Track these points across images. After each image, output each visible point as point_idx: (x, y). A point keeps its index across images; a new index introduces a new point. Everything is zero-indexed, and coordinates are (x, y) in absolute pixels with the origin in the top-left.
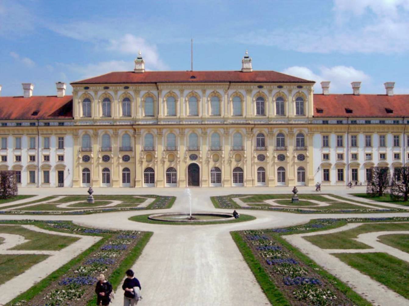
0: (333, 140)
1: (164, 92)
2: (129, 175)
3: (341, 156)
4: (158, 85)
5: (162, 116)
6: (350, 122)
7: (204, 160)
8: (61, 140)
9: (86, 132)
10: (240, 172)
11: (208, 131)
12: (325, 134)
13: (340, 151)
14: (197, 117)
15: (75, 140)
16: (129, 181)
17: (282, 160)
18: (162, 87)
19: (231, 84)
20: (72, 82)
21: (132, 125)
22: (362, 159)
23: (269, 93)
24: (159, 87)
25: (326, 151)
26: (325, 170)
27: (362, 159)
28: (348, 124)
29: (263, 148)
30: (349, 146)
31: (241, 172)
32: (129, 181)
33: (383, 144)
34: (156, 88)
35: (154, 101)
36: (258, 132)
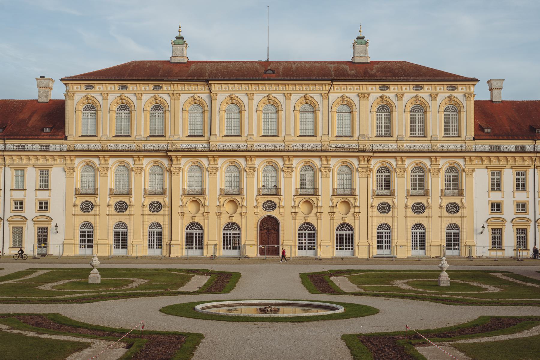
2: (160, 235)
5: (218, 135)
7: (288, 210)
8: (44, 176)
13: (521, 197)
17: (420, 213)
19: (334, 83)
20: (63, 77)
21: (166, 152)
25: (496, 197)
26: (493, 230)
29: (387, 192)
36: (379, 165)
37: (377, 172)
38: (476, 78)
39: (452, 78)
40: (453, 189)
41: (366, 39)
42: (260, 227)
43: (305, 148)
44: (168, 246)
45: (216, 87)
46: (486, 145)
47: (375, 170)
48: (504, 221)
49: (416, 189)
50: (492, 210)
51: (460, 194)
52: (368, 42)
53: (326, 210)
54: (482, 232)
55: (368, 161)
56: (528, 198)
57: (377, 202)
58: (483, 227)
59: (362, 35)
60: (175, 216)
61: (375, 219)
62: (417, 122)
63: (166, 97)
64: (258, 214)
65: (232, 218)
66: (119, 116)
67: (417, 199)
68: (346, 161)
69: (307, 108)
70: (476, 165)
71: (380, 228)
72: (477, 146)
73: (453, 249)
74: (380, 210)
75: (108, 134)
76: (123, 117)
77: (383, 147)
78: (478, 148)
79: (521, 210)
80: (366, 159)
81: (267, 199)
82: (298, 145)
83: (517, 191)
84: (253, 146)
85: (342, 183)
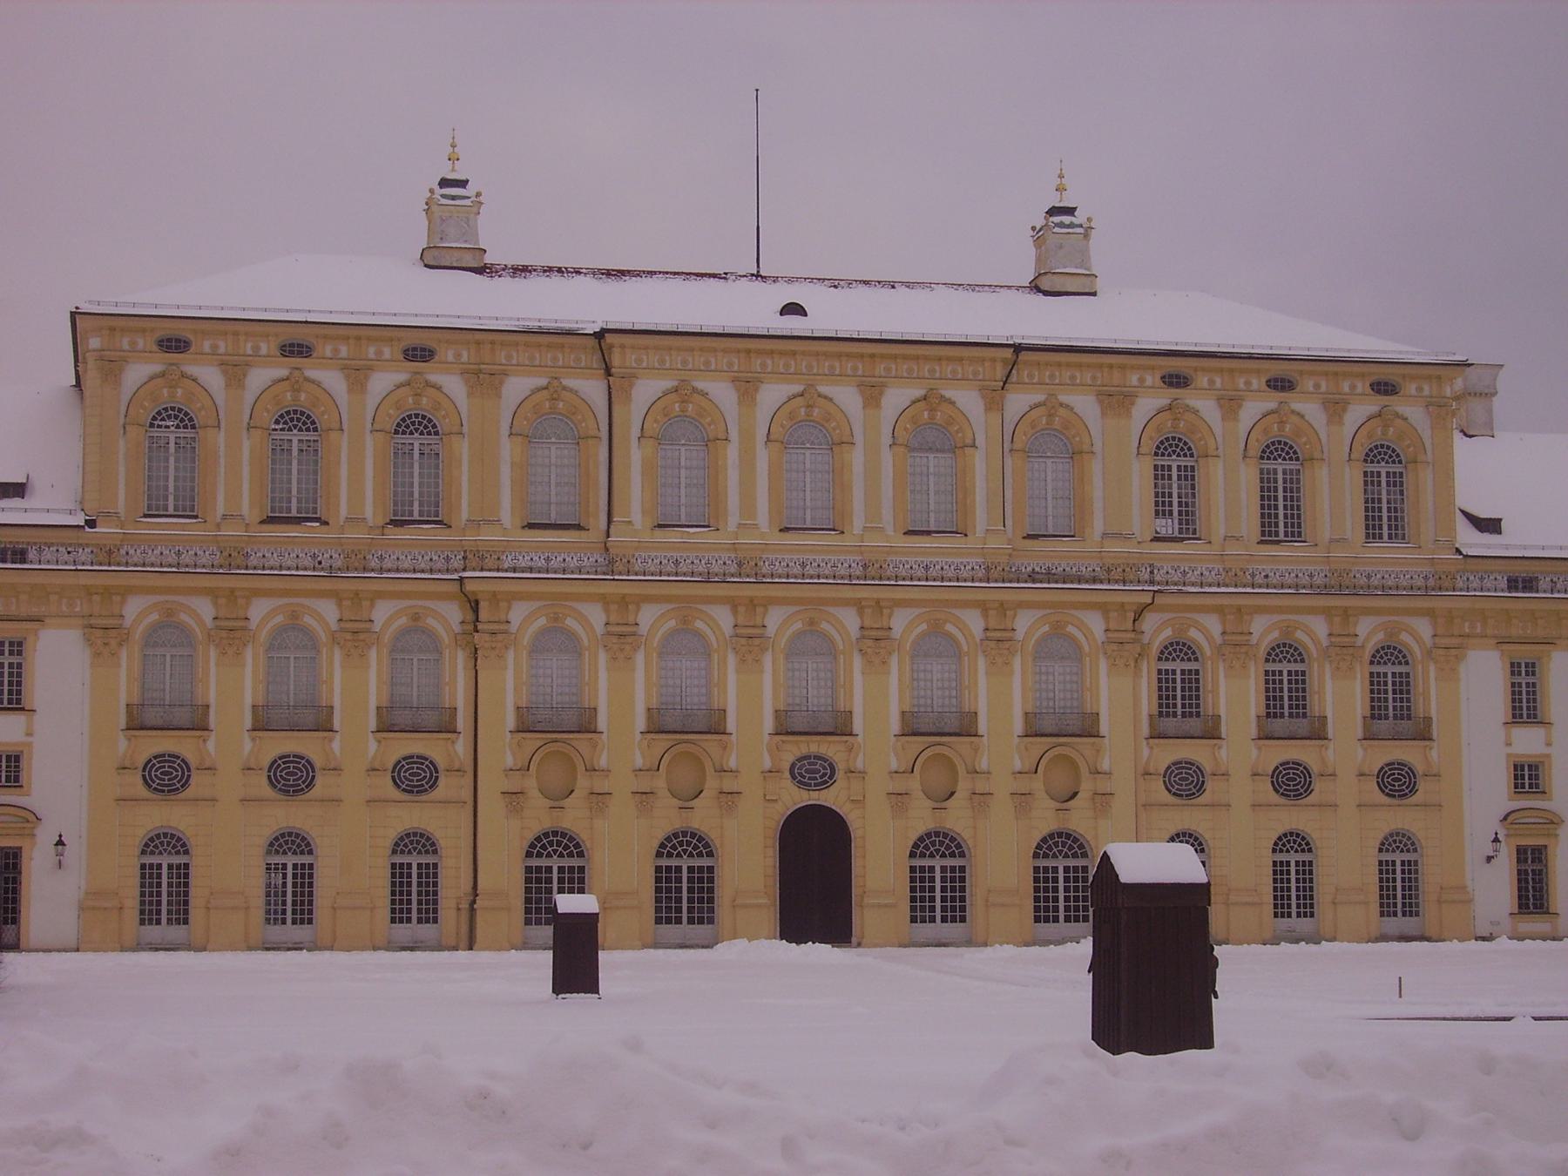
1: (647, 390)
2: (430, 874)
4: (611, 347)
9: (294, 615)
10: (1071, 863)
11: (900, 621)
12: (1524, 653)
14: (831, 539)
15: (97, 654)
16: (429, 914)
17: (1298, 796)
18: (631, 359)
23: (1330, 422)
24: (616, 360)
26: (1521, 852)
32: (429, 914)
34: (596, 361)
35: (580, 440)
36: (1167, 633)
37: (1160, 659)
44: (465, 916)
49: (1282, 715)
54: (1489, 859)
55: (1134, 621)
58: (1496, 840)
60: (490, 805)
62: (1280, 494)
63: (454, 385)
66: (280, 451)
72: (1472, 578)
73: (1400, 914)
74: (1173, 787)
75: (245, 510)
76: (295, 452)
81: (804, 751)
84: (884, 566)
85: (1051, 695)
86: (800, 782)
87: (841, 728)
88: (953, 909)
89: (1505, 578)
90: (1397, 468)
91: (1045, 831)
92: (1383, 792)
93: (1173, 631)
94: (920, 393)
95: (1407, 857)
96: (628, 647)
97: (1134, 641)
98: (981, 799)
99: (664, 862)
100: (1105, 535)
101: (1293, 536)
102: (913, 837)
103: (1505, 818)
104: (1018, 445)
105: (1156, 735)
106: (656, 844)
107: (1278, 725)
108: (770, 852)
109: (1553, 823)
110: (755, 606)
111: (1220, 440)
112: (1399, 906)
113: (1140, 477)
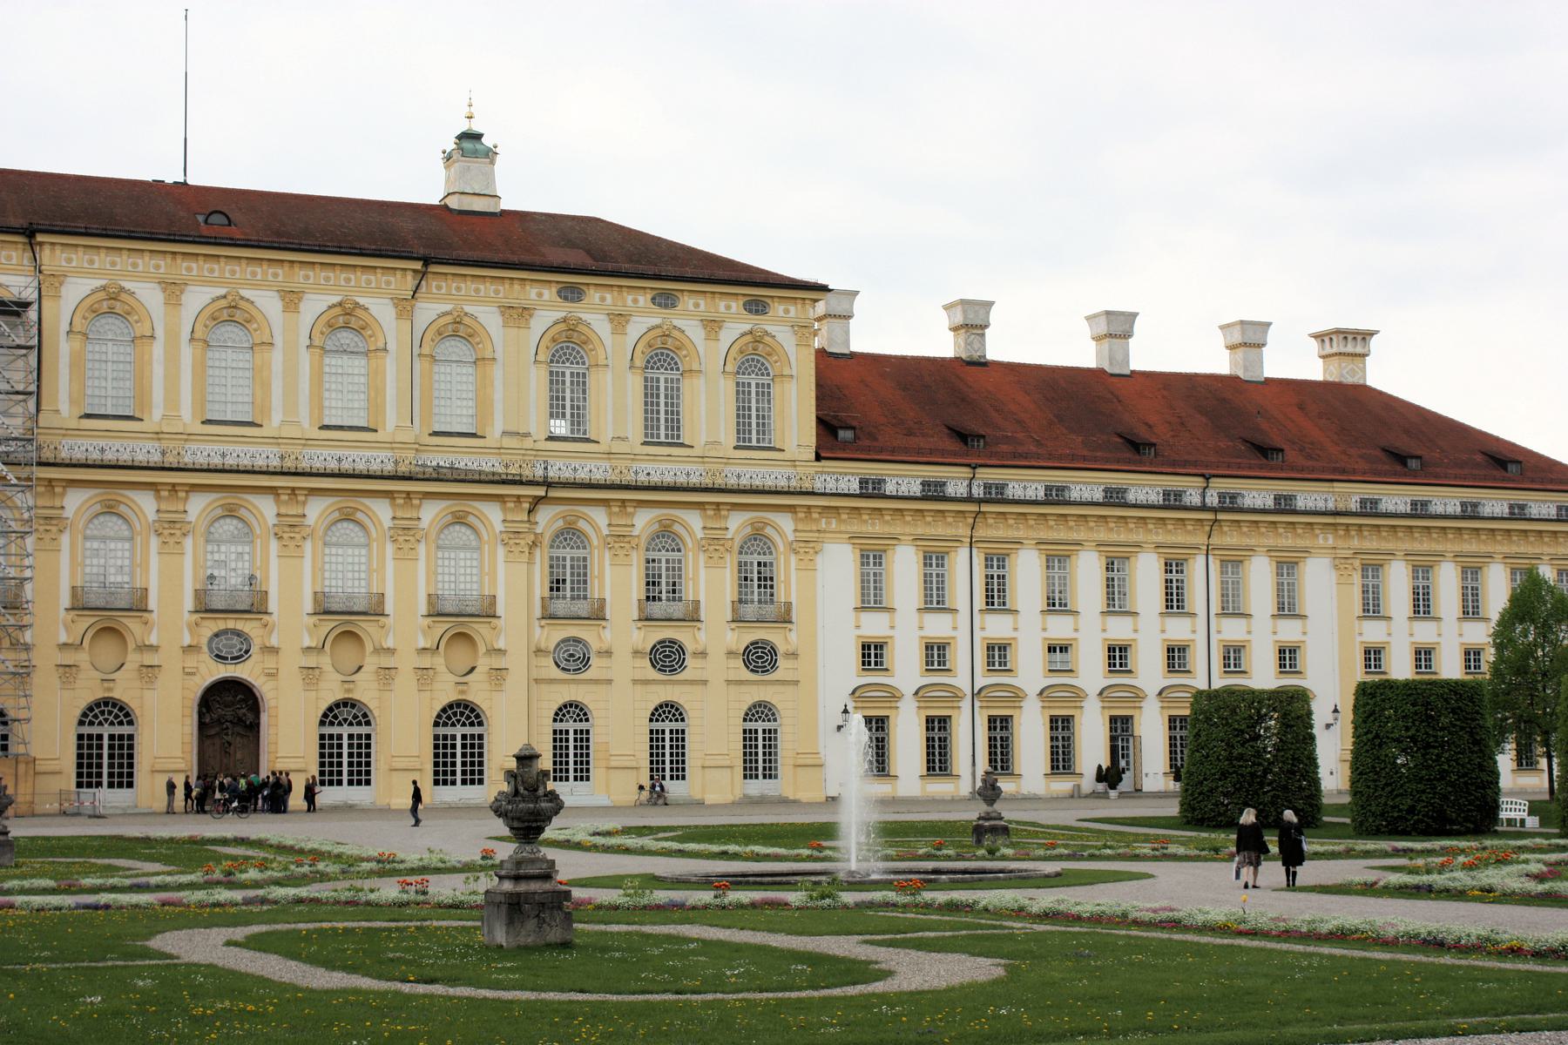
0: (905, 567)
3: (936, 653)
4: (41, 244)
6: (978, 491)
7: (291, 662)
10: (468, 730)
13: (938, 626)
19: (433, 268)
22: (1149, 671)
27: (1149, 671)
28: (969, 499)
30: (1213, 611)
31: (476, 730)
33: (1116, 600)
36: (560, 523)
37: (552, 547)
38: (822, 281)
39: (734, 275)
40: (760, 602)
41: (487, 141)
42: (201, 715)
43: (347, 466)
45: (57, 255)
46: (845, 476)
47: (546, 540)
48: (894, 696)
50: (863, 664)
51: (785, 619)
52: (497, 150)
53: (406, 662)
54: (839, 728)
55: (530, 512)
56: (955, 628)
57: (554, 635)
58: (846, 711)
59: (476, 127)
61: (544, 687)
62: (662, 400)
64: (193, 674)
65: (111, 685)
67: (569, 628)
68: (467, 509)
69: (347, 342)
70: (825, 532)
71: (559, 715)
72: (828, 479)
73: (760, 777)
77: (575, 470)
78: (831, 485)
79: (997, 664)
80: (526, 506)
81: (222, 625)
82: (322, 457)
83: (926, 608)
85: (453, 579)
86: (217, 656)
87: (257, 608)
88: (359, 773)
89: (857, 480)
90: (765, 380)
91: (445, 701)
92: (748, 668)
93: (565, 523)
94: (336, 299)
95: (768, 726)
96: (54, 529)
97: (530, 531)
98: (386, 674)
99: (86, 730)
100: (504, 433)
101: (673, 438)
102: (324, 707)
103: (853, 693)
104: (426, 350)
105: (549, 616)
106: (78, 713)
107: (656, 609)
108: (188, 721)
109: (895, 697)
110: (53, 487)
111: (609, 350)
112: (760, 769)
113: (537, 381)
